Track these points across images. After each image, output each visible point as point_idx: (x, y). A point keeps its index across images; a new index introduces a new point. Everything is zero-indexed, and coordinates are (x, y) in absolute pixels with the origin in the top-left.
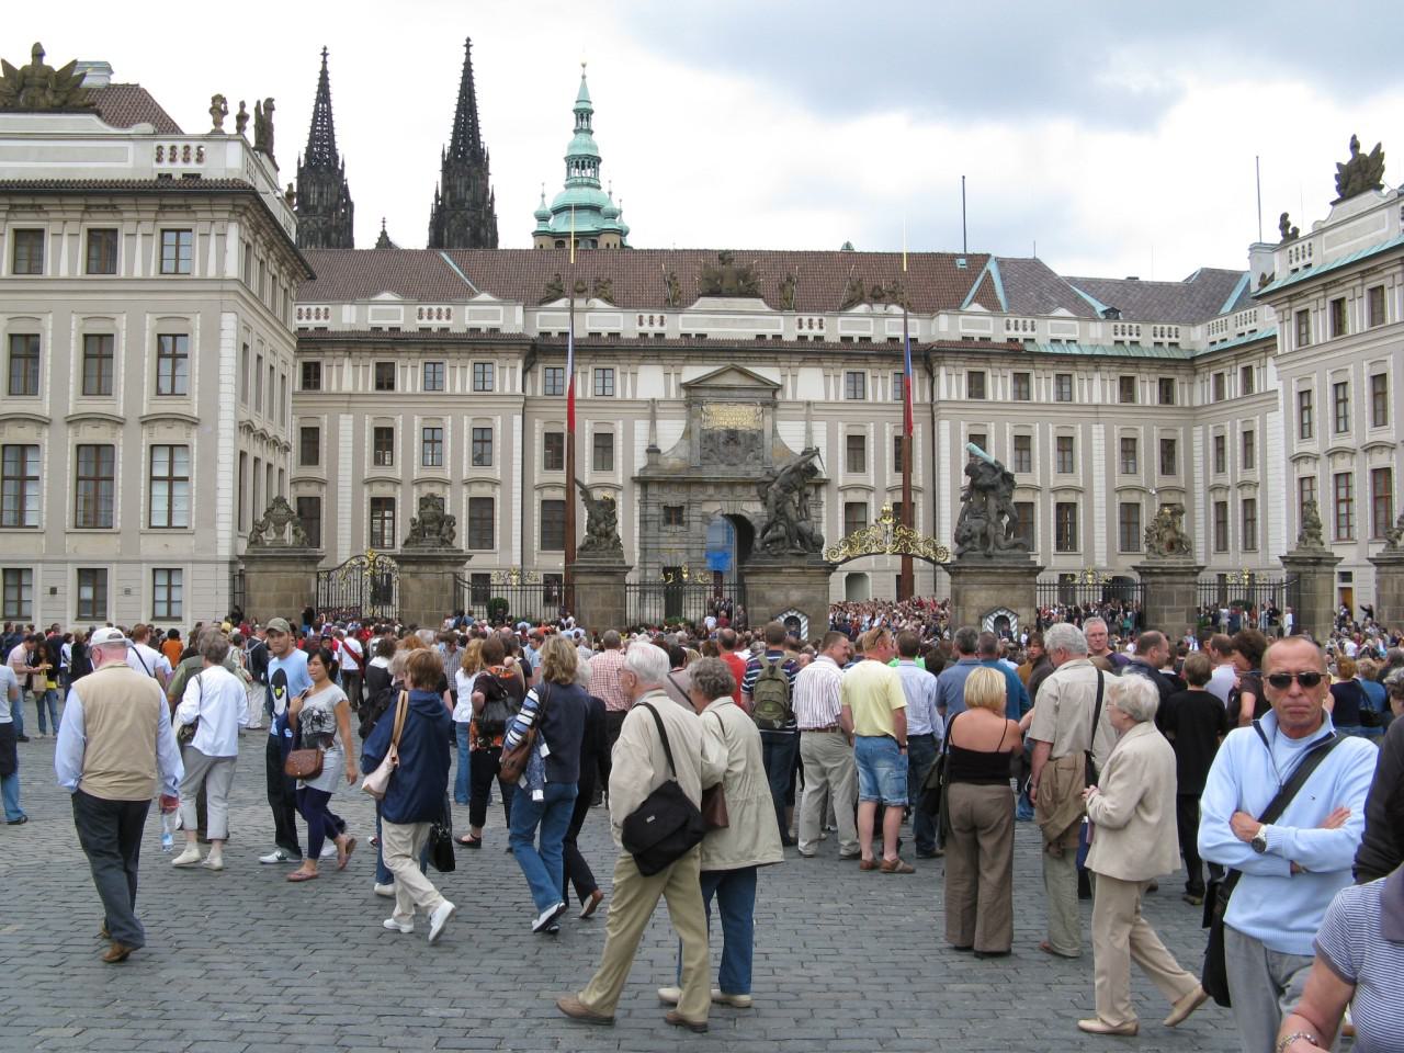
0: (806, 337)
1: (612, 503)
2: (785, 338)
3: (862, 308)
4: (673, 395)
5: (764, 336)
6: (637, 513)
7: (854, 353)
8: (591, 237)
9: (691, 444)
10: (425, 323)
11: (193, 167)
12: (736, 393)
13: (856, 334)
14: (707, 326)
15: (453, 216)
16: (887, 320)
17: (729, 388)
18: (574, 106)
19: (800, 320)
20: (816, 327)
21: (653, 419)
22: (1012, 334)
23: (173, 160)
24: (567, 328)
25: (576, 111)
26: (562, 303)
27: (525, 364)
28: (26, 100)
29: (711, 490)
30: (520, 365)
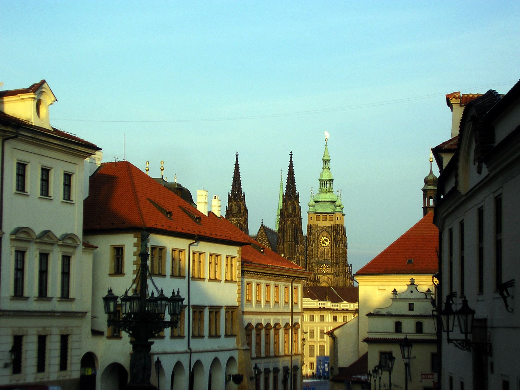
11: (324, 306)
15: (288, 220)
18: (322, 157)
25: (323, 160)
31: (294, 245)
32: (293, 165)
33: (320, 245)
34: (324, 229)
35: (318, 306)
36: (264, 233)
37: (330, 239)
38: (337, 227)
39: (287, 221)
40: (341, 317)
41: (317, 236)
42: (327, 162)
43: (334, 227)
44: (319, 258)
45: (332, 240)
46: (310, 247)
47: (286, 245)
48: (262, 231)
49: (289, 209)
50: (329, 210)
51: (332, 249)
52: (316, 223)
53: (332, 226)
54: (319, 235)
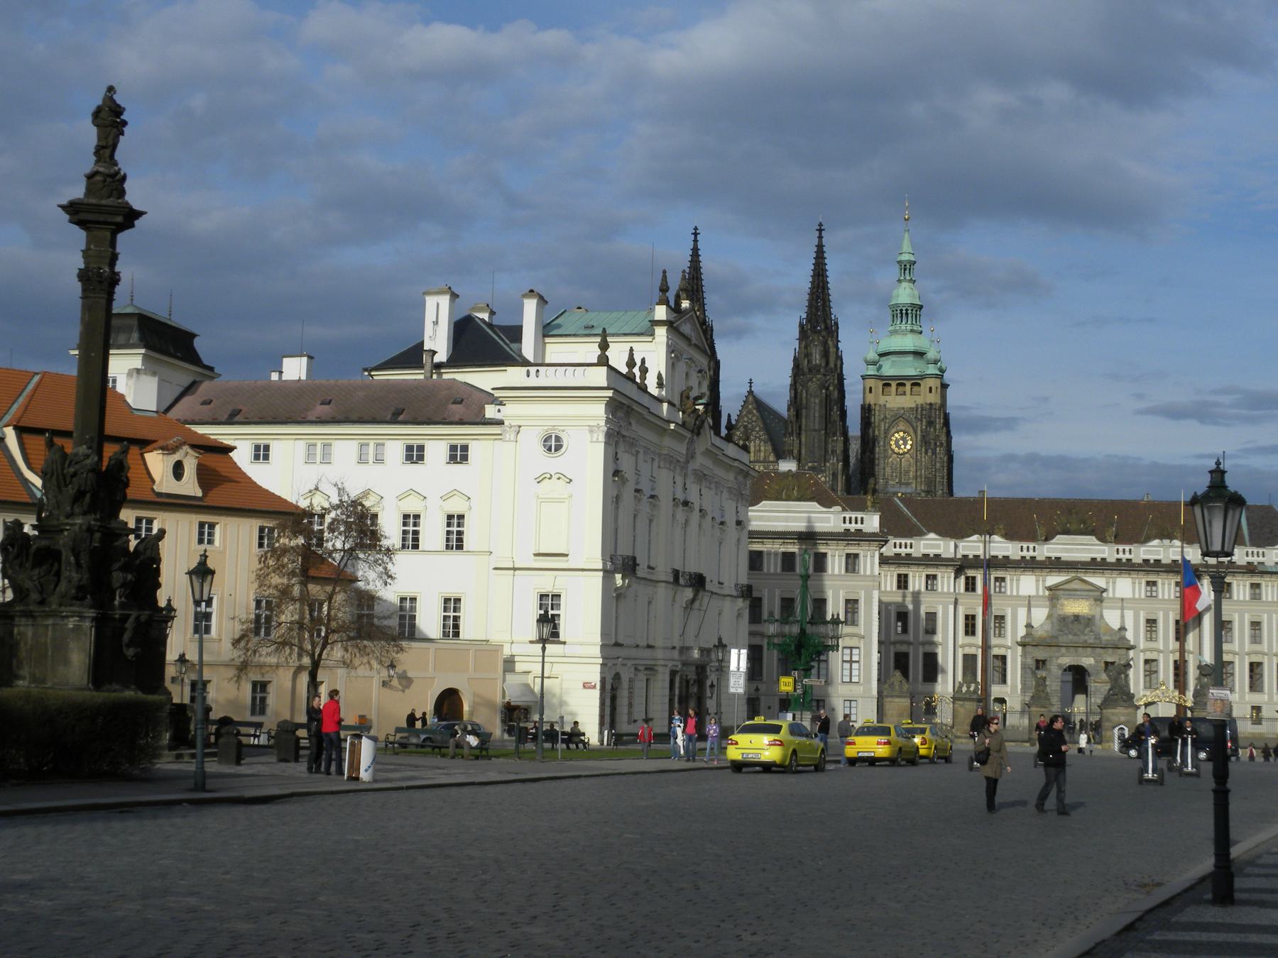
0: (1121, 559)
1: (1003, 658)
2: (1108, 560)
3: (1156, 542)
4: (1041, 593)
5: (1096, 559)
6: (1019, 663)
7: (1153, 567)
8: (916, 382)
9: (1052, 623)
11: (859, 526)
12: (1079, 593)
13: (1152, 557)
16: (1171, 549)
19: (1118, 550)
20: (1127, 553)
22: (1250, 559)
23: (850, 523)
24: (980, 552)
26: (975, 537)
27: (955, 574)
29: (1063, 650)
30: (953, 575)
31: (823, 437)
32: (825, 255)
33: (890, 452)
34: (899, 417)
36: (755, 411)
37: (914, 439)
38: (931, 409)
40: (920, 577)
41: (885, 429)
42: (908, 266)
43: (922, 410)
48: (750, 407)
49: (814, 355)
50: (911, 372)
52: (882, 400)
53: (917, 408)
54: (889, 427)
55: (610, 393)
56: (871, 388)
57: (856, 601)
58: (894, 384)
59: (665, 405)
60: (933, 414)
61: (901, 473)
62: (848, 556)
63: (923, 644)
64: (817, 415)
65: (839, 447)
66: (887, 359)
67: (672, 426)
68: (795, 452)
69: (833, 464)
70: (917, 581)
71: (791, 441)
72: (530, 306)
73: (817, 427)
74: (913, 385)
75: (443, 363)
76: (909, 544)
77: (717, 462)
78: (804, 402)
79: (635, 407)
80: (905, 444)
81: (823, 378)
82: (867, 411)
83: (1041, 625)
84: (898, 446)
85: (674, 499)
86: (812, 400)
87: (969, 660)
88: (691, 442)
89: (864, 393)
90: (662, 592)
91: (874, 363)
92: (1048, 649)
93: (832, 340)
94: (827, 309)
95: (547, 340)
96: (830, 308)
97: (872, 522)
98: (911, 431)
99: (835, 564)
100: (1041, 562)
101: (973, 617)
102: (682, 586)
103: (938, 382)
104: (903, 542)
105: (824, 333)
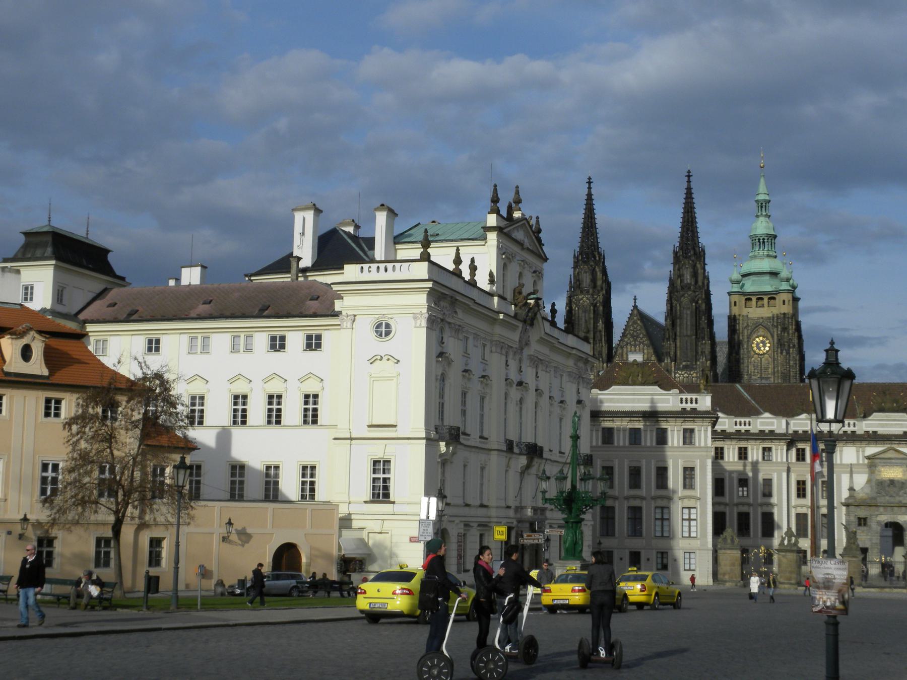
9: (871, 487)
10: (738, 427)
11: (694, 405)
12: (893, 461)
14: (877, 427)
15: (683, 295)
17: (890, 459)
21: (851, 473)
23: (687, 403)
24: (808, 428)
26: (804, 416)
28: (632, 380)
29: (881, 509)
30: (785, 448)
31: (694, 341)
34: (758, 325)
35: (678, 407)
39: (682, 299)
41: (747, 335)
43: (777, 319)
44: (750, 375)
45: (773, 341)
46: (734, 355)
47: (680, 342)
49: (685, 276)
50: (768, 288)
51: (774, 358)
52: (745, 311)
53: (773, 317)
54: (751, 333)
55: (430, 285)
56: (735, 303)
57: (692, 469)
58: (754, 299)
59: (496, 299)
60: (786, 322)
61: (761, 370)
62: (685, 430)
63: (761, 505)
64: (689, 323)
65: (708, 349)
66: (749, 279)
67: (501, 316)
68: (672, 353)
69: (702, 362)
70: (755, 452)
71: (668, 345)
72: (381, 218)
73: (689, 333)
74: (770, 298)
75: (309, 267)
76: (747, 422)
77: (553, 348)
78: (678, 313)
79: (459, 298)
80: (764, 346)
81: (693, 294)
82: (733, 321)
83: (862, 488)
84: (759, 348)
85: (506, 380)
86: (685, 312)
87: (801, 518)
88: (525, 331)
89: (730, 306)
90: (495, 462)
91: (738, 282)
92: (868, 508)
93: (700, 264)
94: (696, 238)
95: (398, 246)
96: (698, 238)
97: (705, 402)
98: (769, 335)
99: (675, 437)
100: (860, 436)
101: (804, 482)
102: (517, 454)
103: (790, 296)
104: (743, 420)
105: (693, 258)
